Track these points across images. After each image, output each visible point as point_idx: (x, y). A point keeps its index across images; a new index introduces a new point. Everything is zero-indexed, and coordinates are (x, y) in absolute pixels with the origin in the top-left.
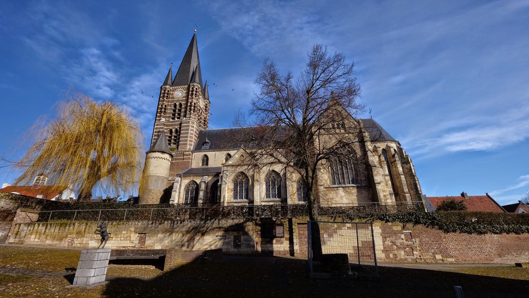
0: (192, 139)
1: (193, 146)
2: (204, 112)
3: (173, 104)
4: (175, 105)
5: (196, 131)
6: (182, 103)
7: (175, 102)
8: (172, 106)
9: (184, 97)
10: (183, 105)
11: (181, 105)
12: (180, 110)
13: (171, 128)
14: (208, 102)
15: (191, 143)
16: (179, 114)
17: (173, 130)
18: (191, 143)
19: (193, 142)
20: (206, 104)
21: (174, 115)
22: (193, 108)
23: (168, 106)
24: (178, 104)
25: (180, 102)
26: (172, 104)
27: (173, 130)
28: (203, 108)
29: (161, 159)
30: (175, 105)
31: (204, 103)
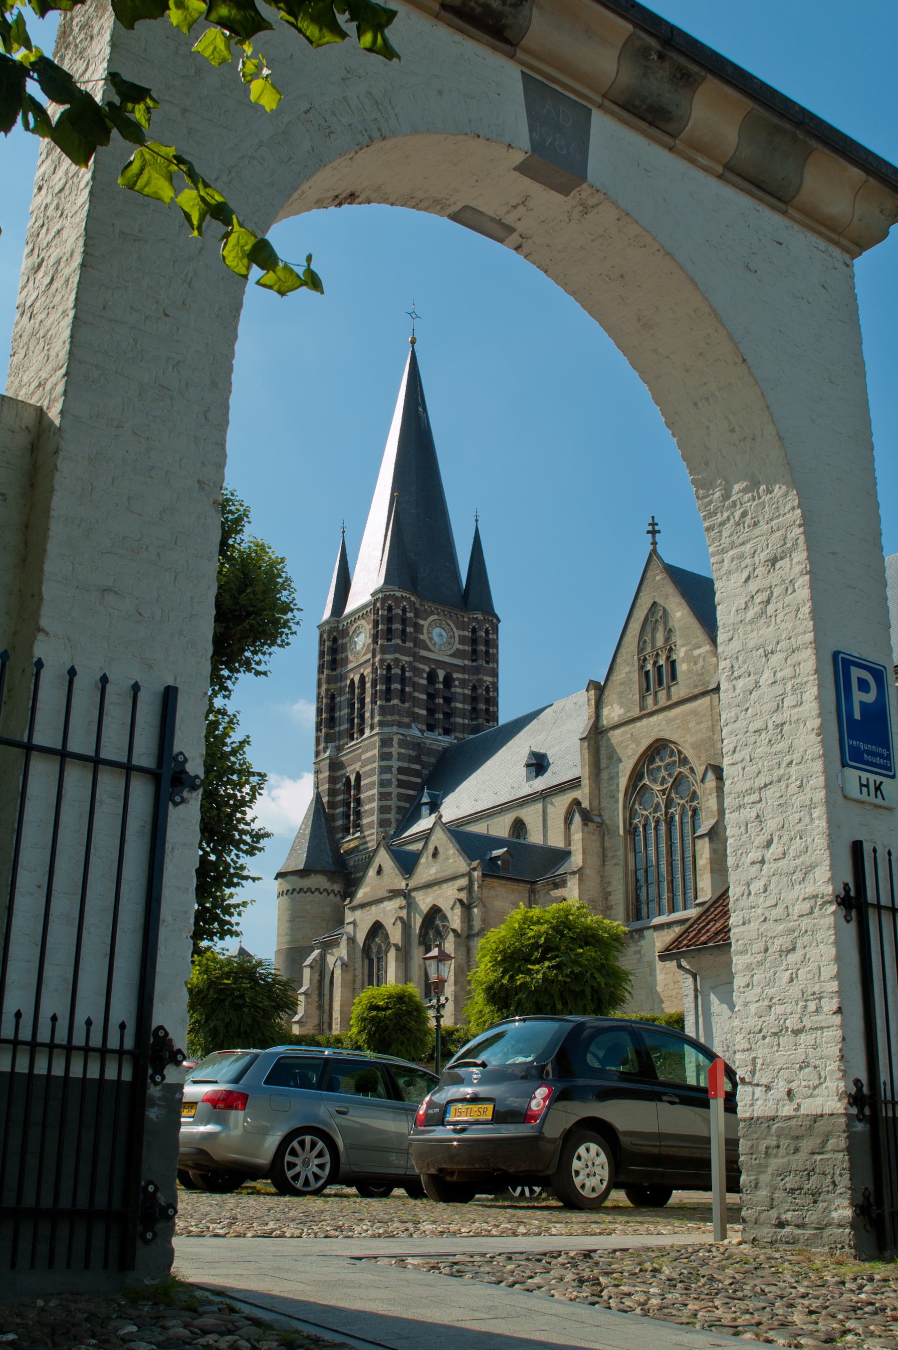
0: (389, 803)
1: (394, 825)
2: (466, 662)
5: (406, 765)
14: (480, 617)
15: (387, 816)
17: (353, 778)
18: (387, 816)
19: (393, 811)
20: (474, 631)
22: (384, 687)
23: (341, 695)
24: (357, 679)
27: (353, 778)
28: (457, 654)
29: (302, 894)
31: (457, 633)
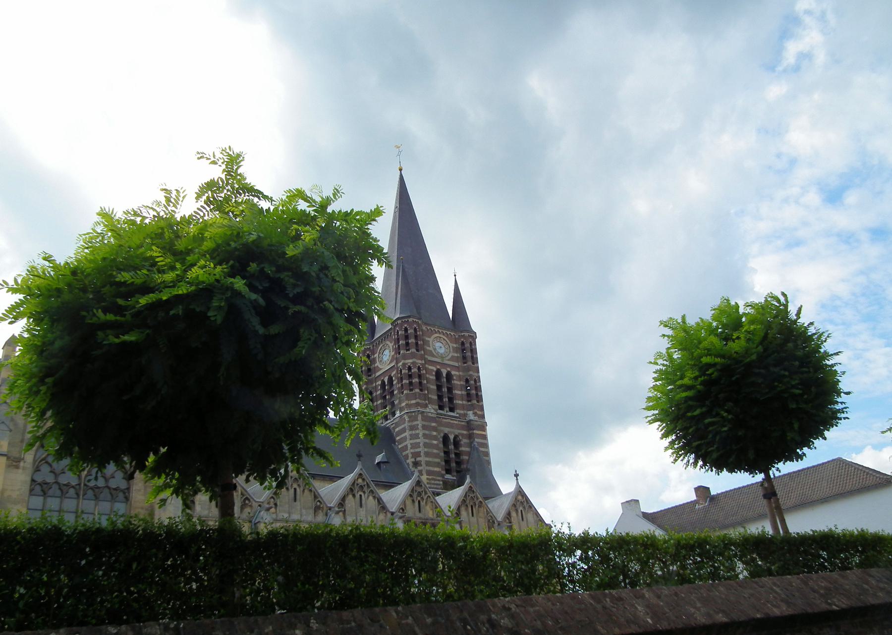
3: (435, 369)
4: (438, 374)
6: (453, 373)
7: (438, 367)
8: (434, 373)
9: (453, 359)
10: (455, 378)
11: (449, 376)
12: (450, 390)
13: (446, 430)
16: (451, 400)
17: (452, 437)
21: (440, 398)
25: (449, 369)
26: (433, 370)
27: (452, 437)
30: (438, 374)
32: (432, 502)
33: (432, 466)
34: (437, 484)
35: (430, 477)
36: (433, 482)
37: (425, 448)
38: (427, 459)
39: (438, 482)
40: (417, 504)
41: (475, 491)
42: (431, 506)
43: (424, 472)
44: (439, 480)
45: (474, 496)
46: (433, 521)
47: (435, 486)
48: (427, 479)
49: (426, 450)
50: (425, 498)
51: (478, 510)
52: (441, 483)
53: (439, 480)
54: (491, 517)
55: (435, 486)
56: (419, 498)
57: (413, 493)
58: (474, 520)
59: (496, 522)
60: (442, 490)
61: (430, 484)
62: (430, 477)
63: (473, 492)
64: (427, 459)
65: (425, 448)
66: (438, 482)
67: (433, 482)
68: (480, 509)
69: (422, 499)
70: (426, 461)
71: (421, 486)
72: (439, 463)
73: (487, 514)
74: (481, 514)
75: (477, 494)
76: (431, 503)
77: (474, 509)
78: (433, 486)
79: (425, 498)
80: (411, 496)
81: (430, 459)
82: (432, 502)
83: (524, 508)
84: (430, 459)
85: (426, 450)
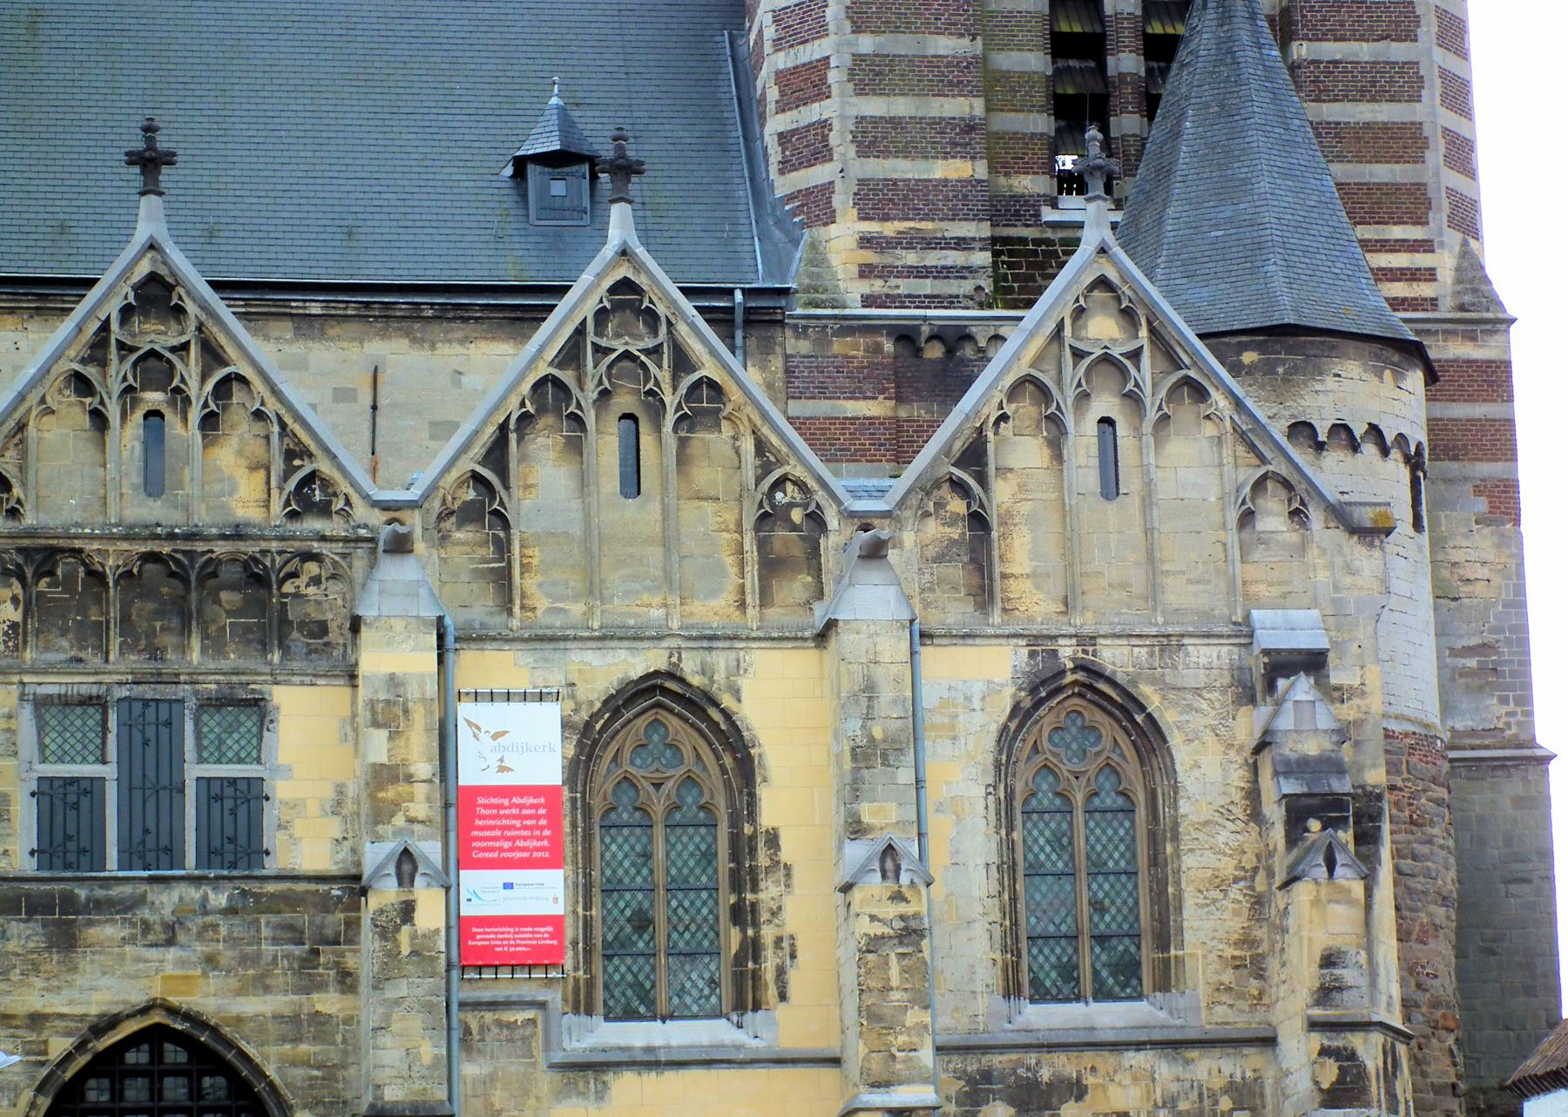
32: (259, 415)
33: (905, 152)
34: (944, 273)
35: (890, 229)
36: (911, 258)
37: (857, 30)
38: (874, 107)
39: (954, 258)
40: (127, 436)
41: (661, 310)
42: (257, 449)
43: (841, 200)
44: (961, 244)
45: (655, 352)
46: (251, 548)
47: (927, 286)
48: (866, 242)
49: (866, 44)
50: (199, 390)
51: (683, 443)
52: (983, 258)
53: (961, 244)
54: (801, 485)
55: (927, 286)
56: (154, 398)
57: (103, 363)
58: (643, 515)
59: (832, 521)
60: (981, 306)
61: (885, 272)
62: (890, 229)
63: (651, 317)
64: (874, 107)
65: (857, 30)
66: (954, 258)
67: (911, 258)
68: (701, 436)
69: (180, 398)
70: (860, 120)
71: (179, 311)
72: (969, 127)
73: (766, 469)
74: (705, 475)
75: (682, 329)
76: (258, 428)
77: (647, 440)
78: (905, 286)
79: (199, 390)
80: (81, 384)
81: (902, 107)
82: (259, 415)
83: (1133, 399)
84: (902, 107)
85: (866, 44)
